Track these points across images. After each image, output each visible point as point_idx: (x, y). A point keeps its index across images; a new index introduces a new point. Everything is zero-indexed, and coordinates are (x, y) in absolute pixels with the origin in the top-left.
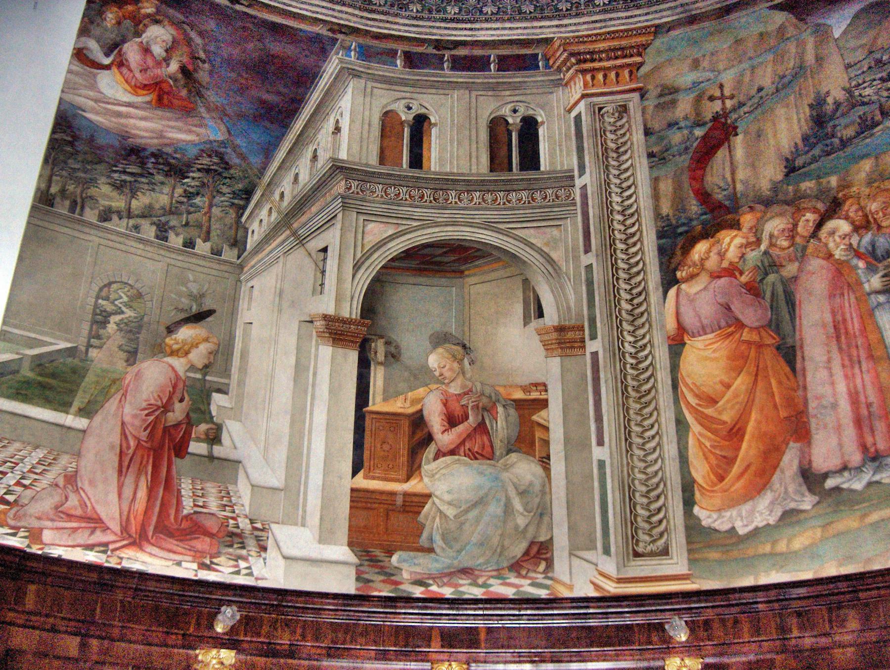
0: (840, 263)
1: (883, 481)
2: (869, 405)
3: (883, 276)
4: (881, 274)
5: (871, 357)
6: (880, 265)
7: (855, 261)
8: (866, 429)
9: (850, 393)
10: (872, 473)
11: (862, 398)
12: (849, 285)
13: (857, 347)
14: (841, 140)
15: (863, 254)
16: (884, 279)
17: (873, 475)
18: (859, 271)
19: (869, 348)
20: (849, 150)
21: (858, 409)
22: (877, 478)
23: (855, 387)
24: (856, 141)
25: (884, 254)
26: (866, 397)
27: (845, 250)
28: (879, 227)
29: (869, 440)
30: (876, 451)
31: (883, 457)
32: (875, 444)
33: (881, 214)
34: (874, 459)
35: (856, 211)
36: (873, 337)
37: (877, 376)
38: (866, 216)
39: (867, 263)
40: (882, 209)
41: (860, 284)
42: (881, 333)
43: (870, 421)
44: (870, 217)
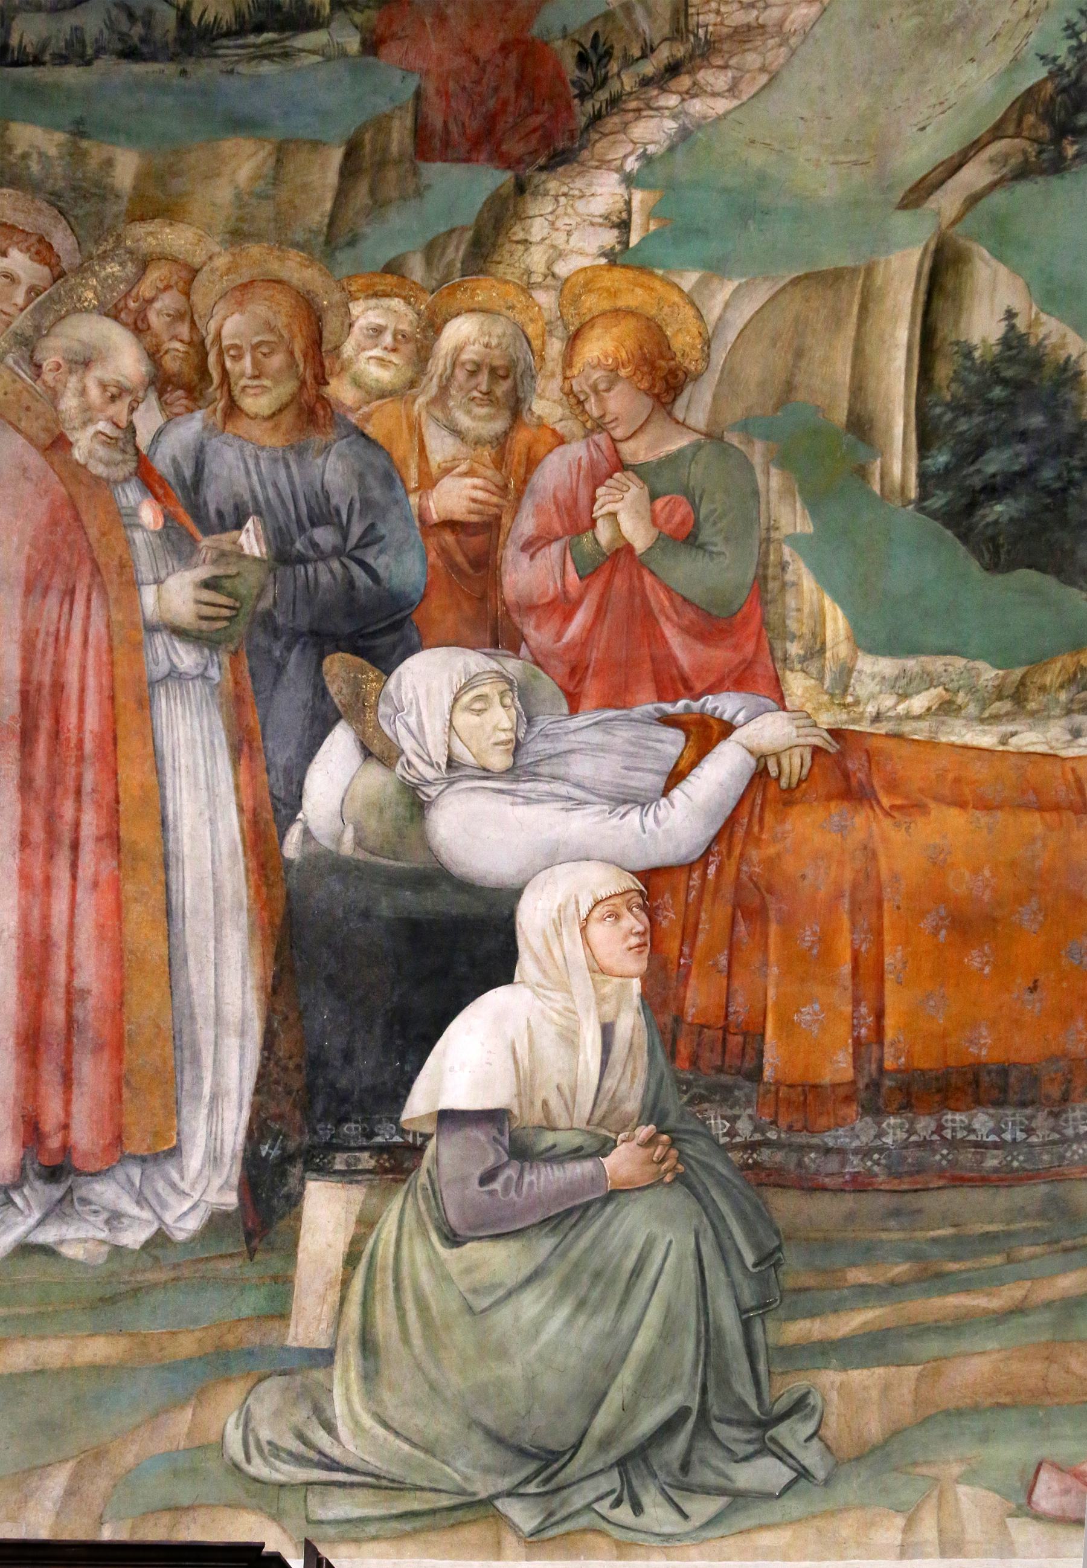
0: (77, 473)
1: (67, 1251)
2: (72, 996)
3: (209, 584)
4: (204, 572)
5: (113, 839)
6: (205, 542)
7: (131, 495)
8: (50, 1073)
9: (25, 934)
10: (37, 1215)
11: (60, 973)
12: (96, 570)
13: (78, 792)
14: (183, 19)
15: (162, 480)
16: (207, 595)
17: (40, 1223)
18: (138, 536)
19: (113, 811)
20: (204, 71)
21: (40, 996)
22: (48, 1235)
23: (46, 918)
24: (228, 48)
25: (228, 509)
26: (71, 971)
27: (110, 442)
28: (233, 409)
29: (52, 1112)
30: (66, 1148)
31: (79, 1173)
32: (66, 1127)
33: (247, 362)
34: (53, 1174)
35: (178, 317)
36: (132, 776)
37: (119, 910)
38: (199, 347)
39: (169, 517)
40: (255, 347)
41: (134, 585)
42: (159, 770)
43: (69, 1054)
44: (212, 359)
